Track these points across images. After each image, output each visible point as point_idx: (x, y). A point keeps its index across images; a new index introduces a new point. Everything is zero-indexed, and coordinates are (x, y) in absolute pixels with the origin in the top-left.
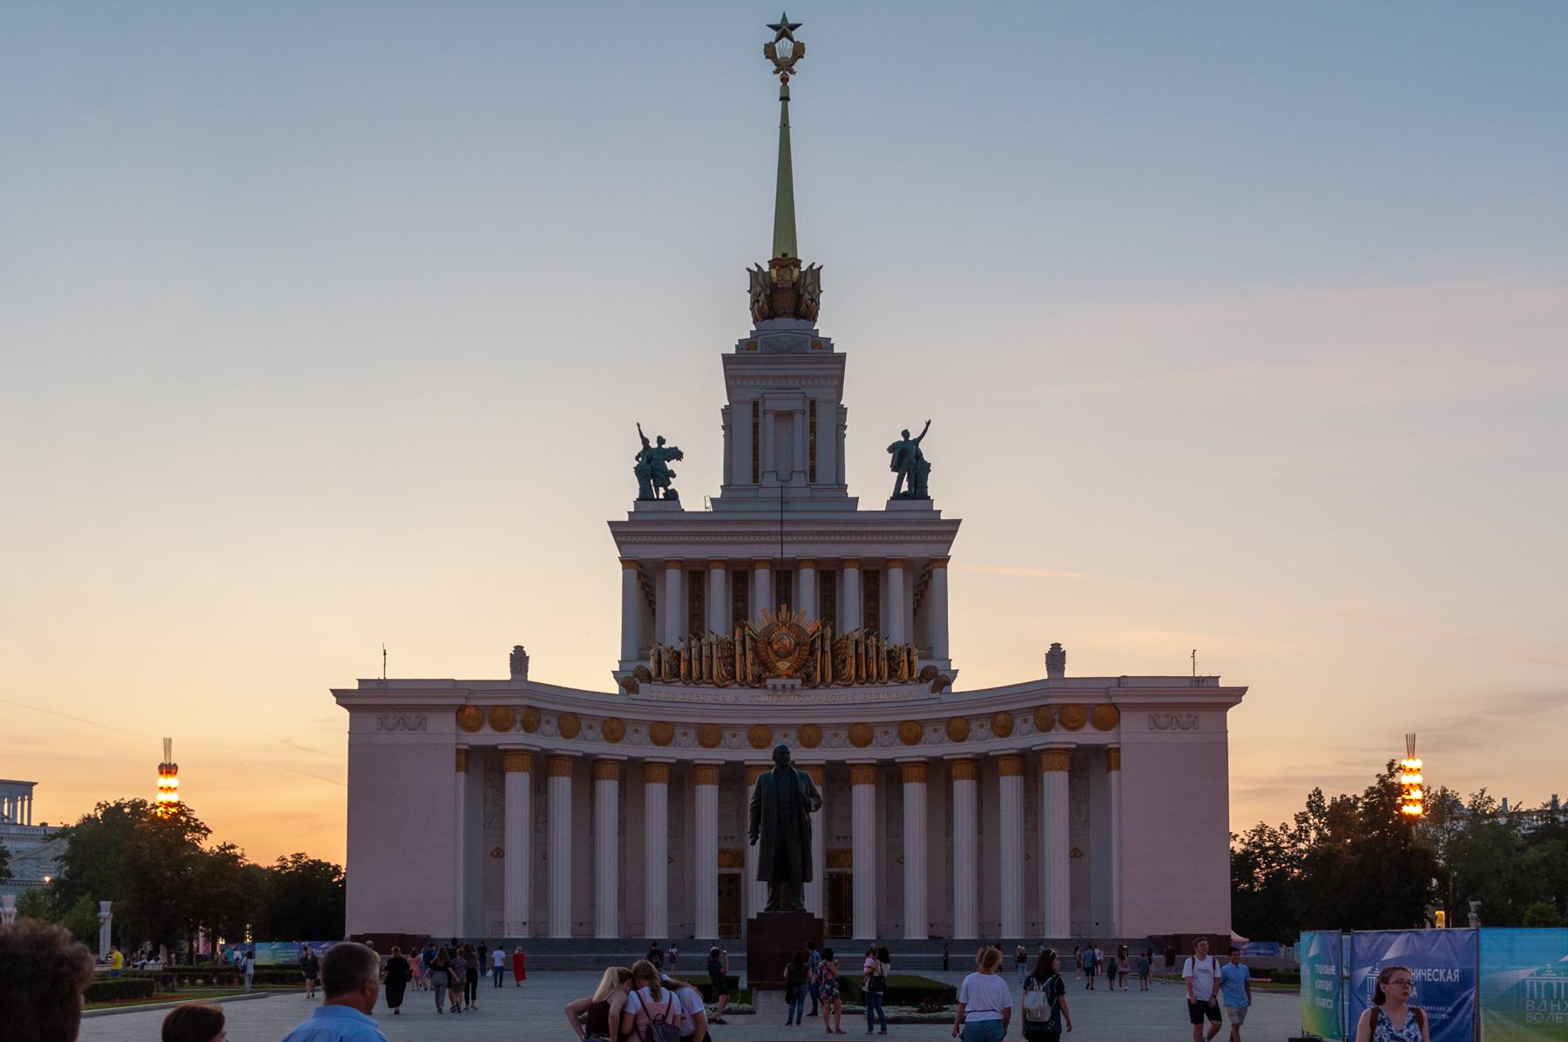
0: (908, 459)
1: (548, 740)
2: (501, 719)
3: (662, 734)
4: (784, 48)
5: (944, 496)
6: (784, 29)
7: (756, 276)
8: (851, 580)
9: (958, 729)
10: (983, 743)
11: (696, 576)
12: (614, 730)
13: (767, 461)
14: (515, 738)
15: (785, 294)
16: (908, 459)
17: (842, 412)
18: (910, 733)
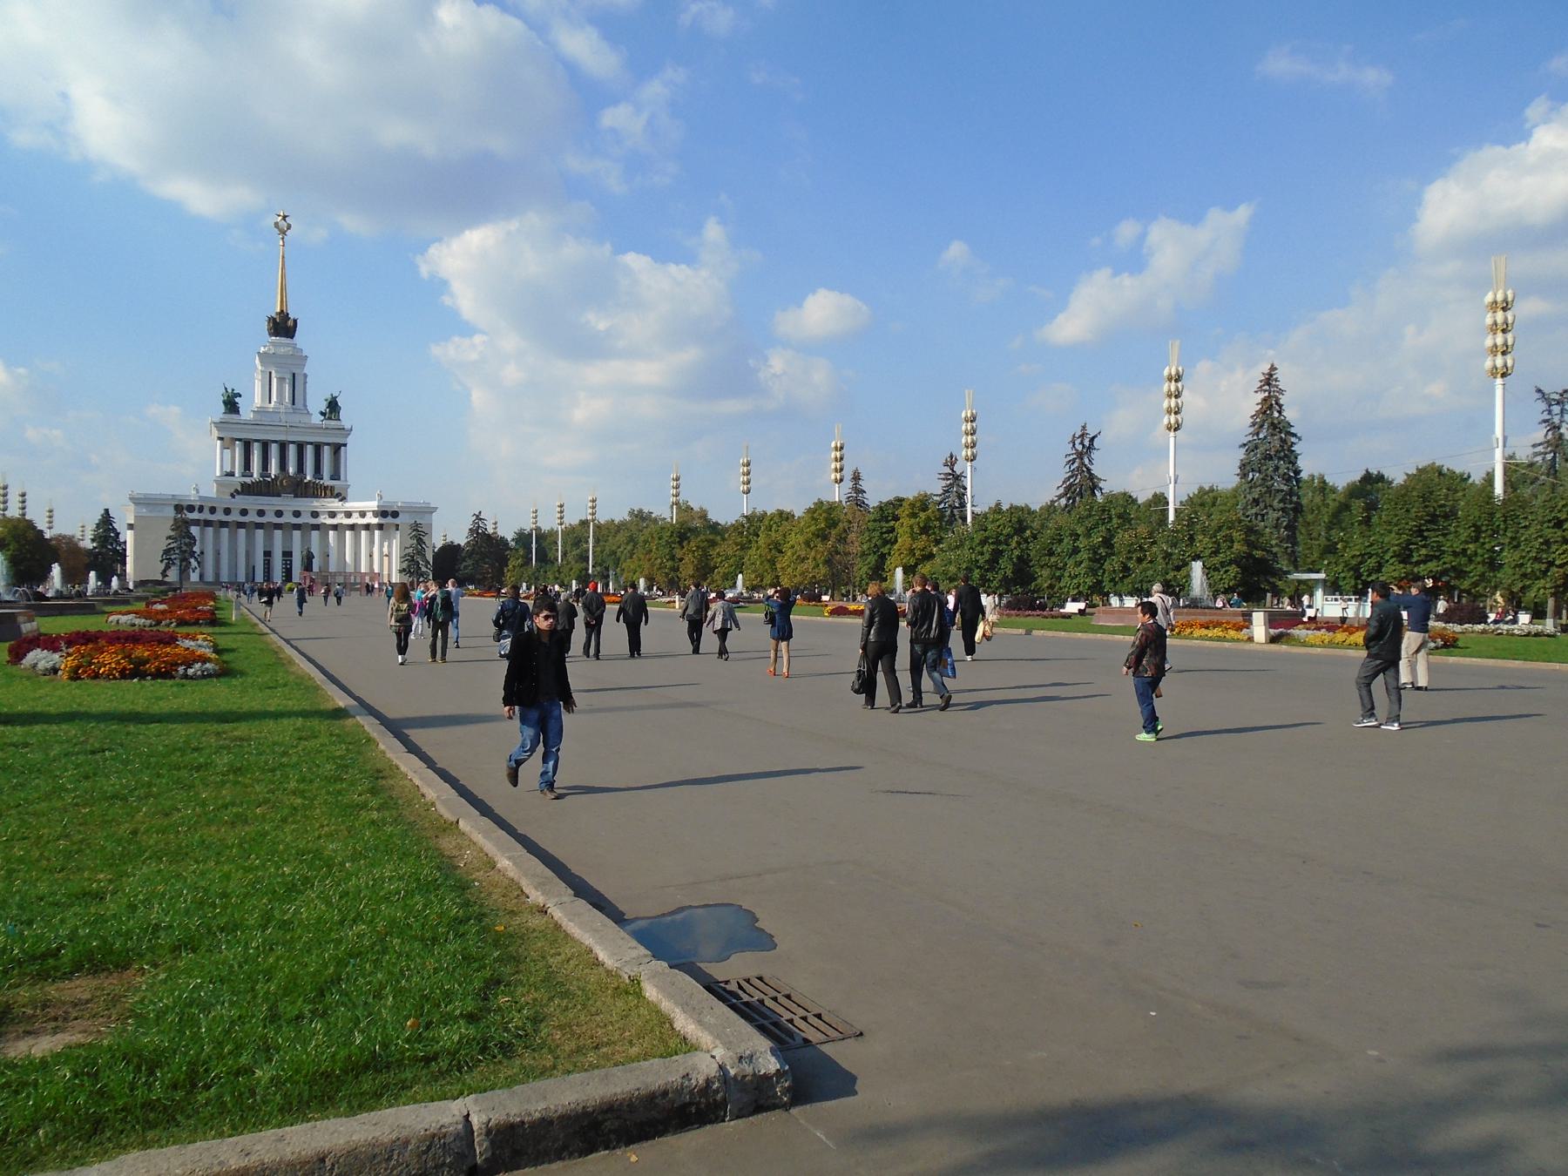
0: (333, 407)
1: (206, 516)
2: (191, 508)
3: (244, 512)
4: (283, 225)
5: (346, 418)
6: (284, 217)
7: (272, 320)
8: (309, 450)
9: (349, 515)
10: (356, 519)
11: (247, 445)
12: (227, 511)
13: (274, 398)
14: (195, 515)
15: (283, 327)
16: (333, 407)
17: (305, 376)
18: (333, 515)
